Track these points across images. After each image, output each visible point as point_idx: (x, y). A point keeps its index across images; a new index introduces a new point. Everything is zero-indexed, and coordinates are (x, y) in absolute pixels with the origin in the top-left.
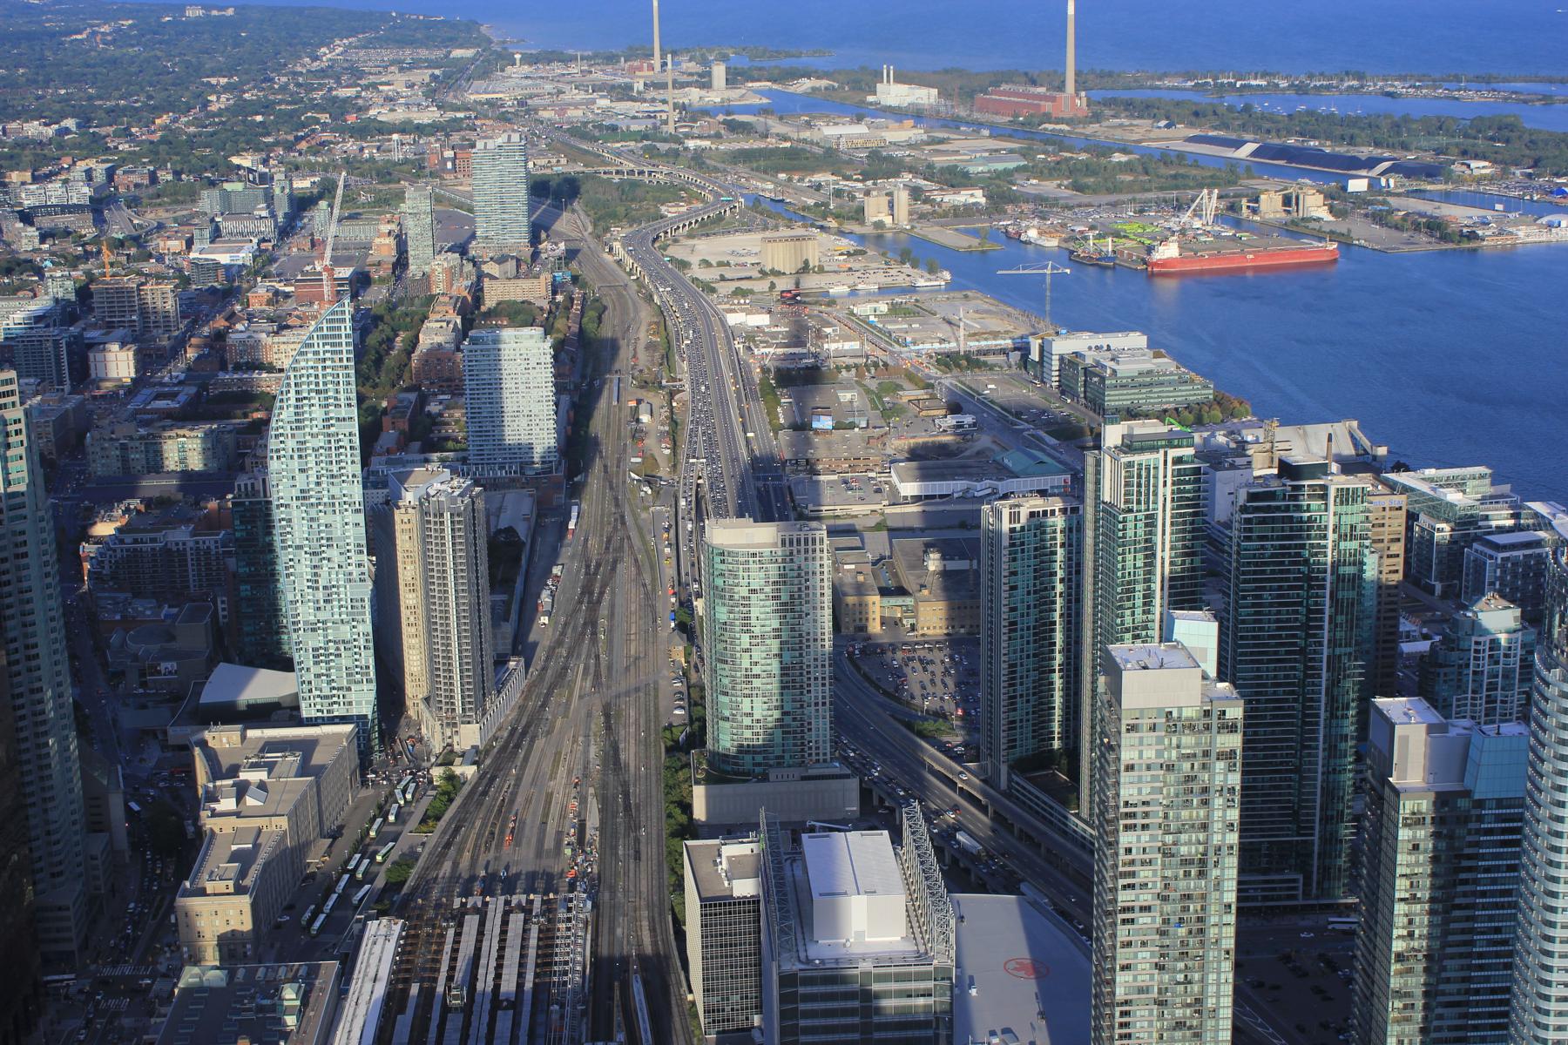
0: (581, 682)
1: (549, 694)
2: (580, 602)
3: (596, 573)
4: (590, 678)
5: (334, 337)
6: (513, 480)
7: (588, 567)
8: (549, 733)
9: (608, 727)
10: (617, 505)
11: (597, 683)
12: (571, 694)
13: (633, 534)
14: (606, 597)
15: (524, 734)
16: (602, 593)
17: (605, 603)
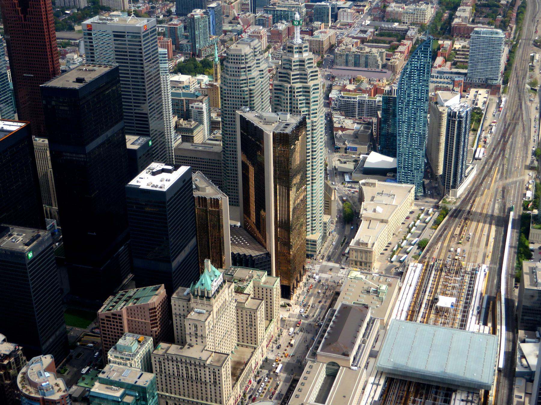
0: (496, 175)
1: (484, 179)
2: (500, 141)
3: (508, 128)
4: (499, 174)
5: (425, 52)
6: (482, 84)
7: (505, 125)
8: (482, 195)
9: (503, 197)
10: (520, 99)
11: (501, 178)
12: (492, 179)
13: (524, 112)
14: (511, 139)
15: (473, 194)
16: (509, 138)
17: (509, 142)
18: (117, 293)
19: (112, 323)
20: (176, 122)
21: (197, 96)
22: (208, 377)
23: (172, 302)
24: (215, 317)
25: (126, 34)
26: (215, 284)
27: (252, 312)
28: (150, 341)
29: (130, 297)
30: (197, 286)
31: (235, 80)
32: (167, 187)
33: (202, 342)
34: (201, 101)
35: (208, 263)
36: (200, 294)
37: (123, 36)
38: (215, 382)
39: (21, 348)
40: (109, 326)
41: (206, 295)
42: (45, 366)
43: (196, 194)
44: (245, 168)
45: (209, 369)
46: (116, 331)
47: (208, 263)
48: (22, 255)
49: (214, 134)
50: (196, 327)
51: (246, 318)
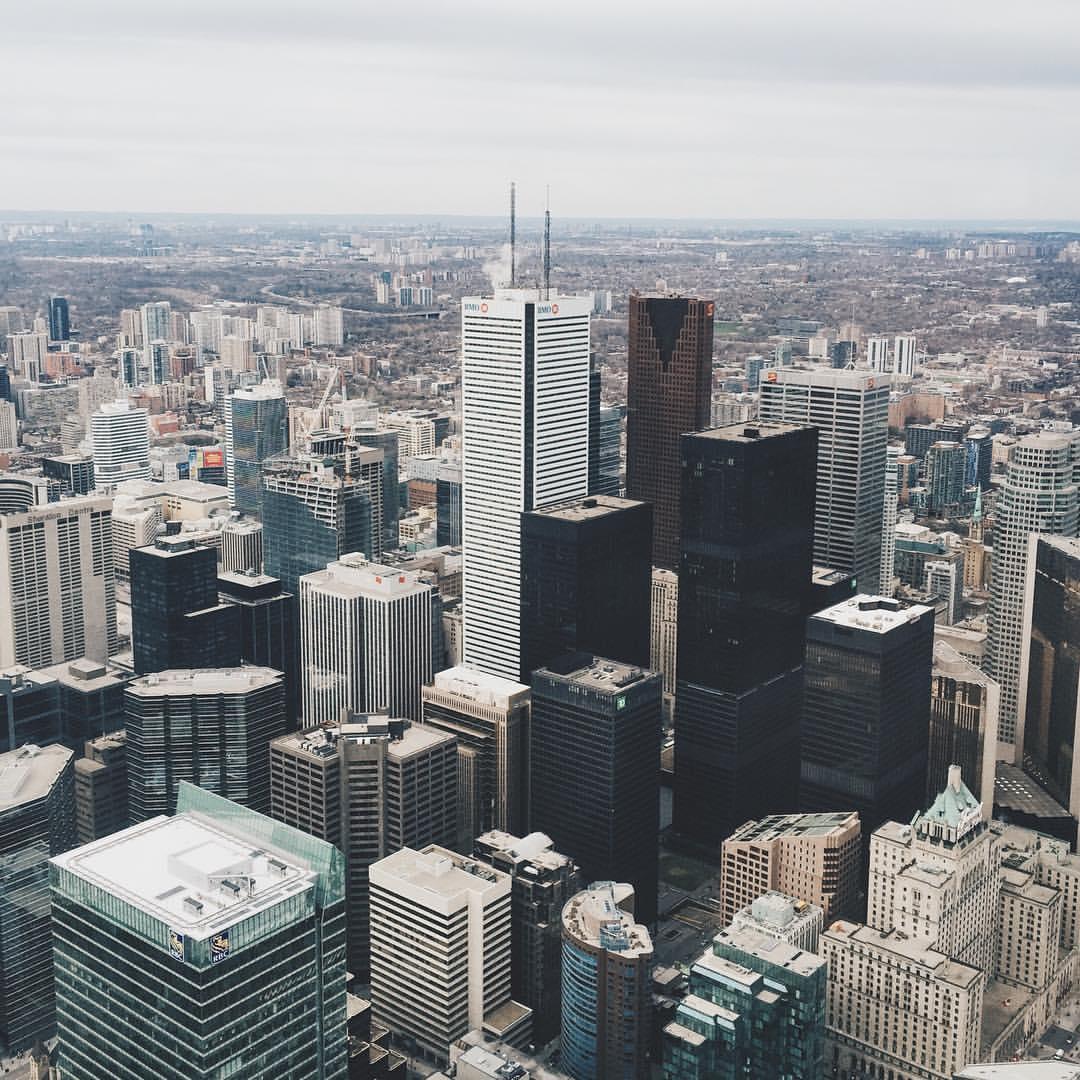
18: (764, 816)
19: (748, 866)
20: (897, 589)
21: (941, 552)
22: (931, 1004)
23: (873, 842)
24: (958, 887)
25: (836, 392)
26: (966, 819)
27: (1035, 908)
28: (817, 912)
29: (789, 825)
30: (927, 815)
31: (1028, 495)
32: (886, 627)
33: (927, 932)
34: (948, 560)
35: (954, 773)
36: (931, 834)
37: (831, 396)
38: (946, 1023)
39: (576, 868)
40: (742, 872)
41: (945, 837)
42: (617, 901)
43: (936, 672)
44: (1035, 646)
45: (937, 988)
46: (754, 884)
47: (954, 773)
48: (608, 700)
49: (967, 620)
50: (917, 896)
51: (1021, 919)
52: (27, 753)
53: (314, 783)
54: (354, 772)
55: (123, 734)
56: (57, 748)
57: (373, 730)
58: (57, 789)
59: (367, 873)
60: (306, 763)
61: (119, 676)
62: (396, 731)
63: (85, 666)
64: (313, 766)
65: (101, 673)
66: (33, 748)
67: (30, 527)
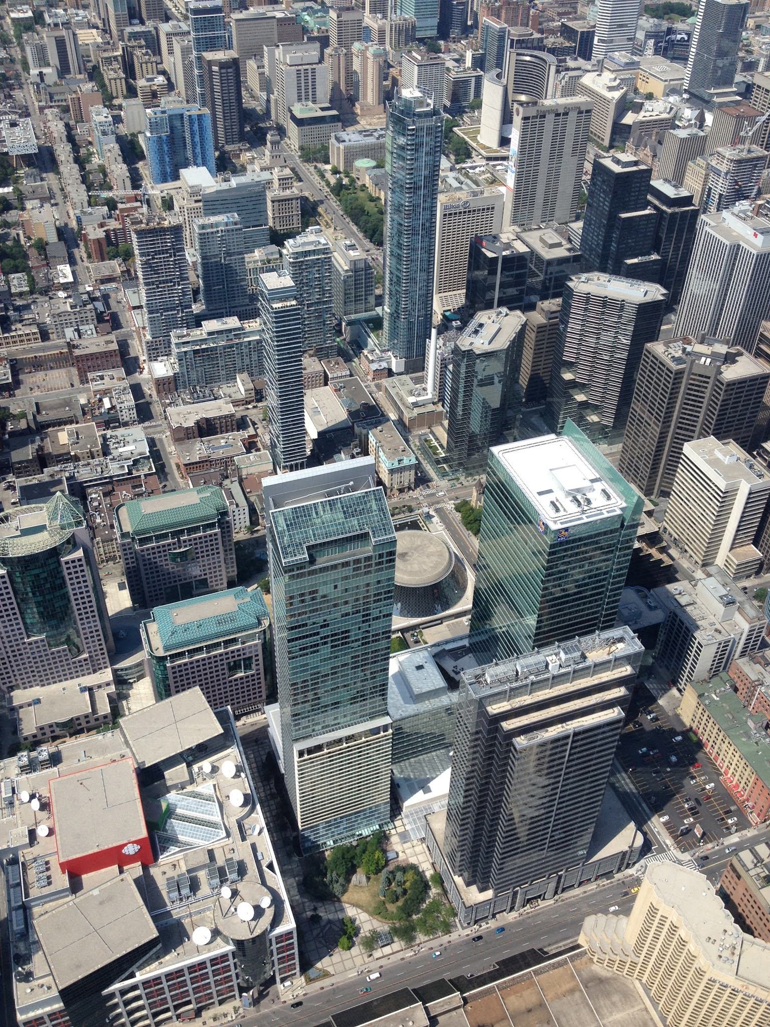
52: (501, 313)
53: (665, 379)
54: (693, 385)
55: (559, 300)
56: (518, 312)
57: (714, 356)
58: (513, 342)
59: (683, 445)
60: (664, 366)
61: (569, 250)
62: (730, 359)
63: (550, 237)
64: (668, 369)
65: (559, 245)
66: (504, 310)
67: (536, 117)
